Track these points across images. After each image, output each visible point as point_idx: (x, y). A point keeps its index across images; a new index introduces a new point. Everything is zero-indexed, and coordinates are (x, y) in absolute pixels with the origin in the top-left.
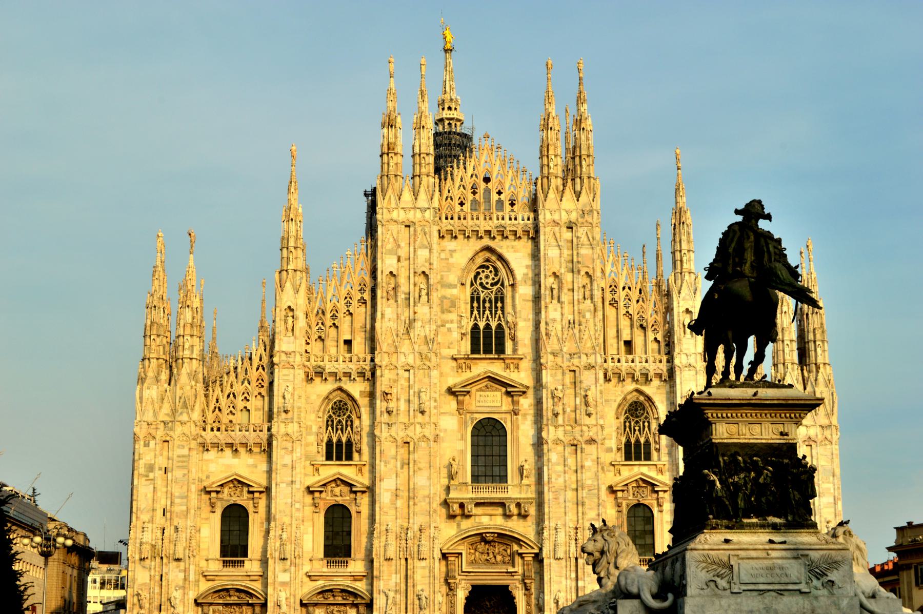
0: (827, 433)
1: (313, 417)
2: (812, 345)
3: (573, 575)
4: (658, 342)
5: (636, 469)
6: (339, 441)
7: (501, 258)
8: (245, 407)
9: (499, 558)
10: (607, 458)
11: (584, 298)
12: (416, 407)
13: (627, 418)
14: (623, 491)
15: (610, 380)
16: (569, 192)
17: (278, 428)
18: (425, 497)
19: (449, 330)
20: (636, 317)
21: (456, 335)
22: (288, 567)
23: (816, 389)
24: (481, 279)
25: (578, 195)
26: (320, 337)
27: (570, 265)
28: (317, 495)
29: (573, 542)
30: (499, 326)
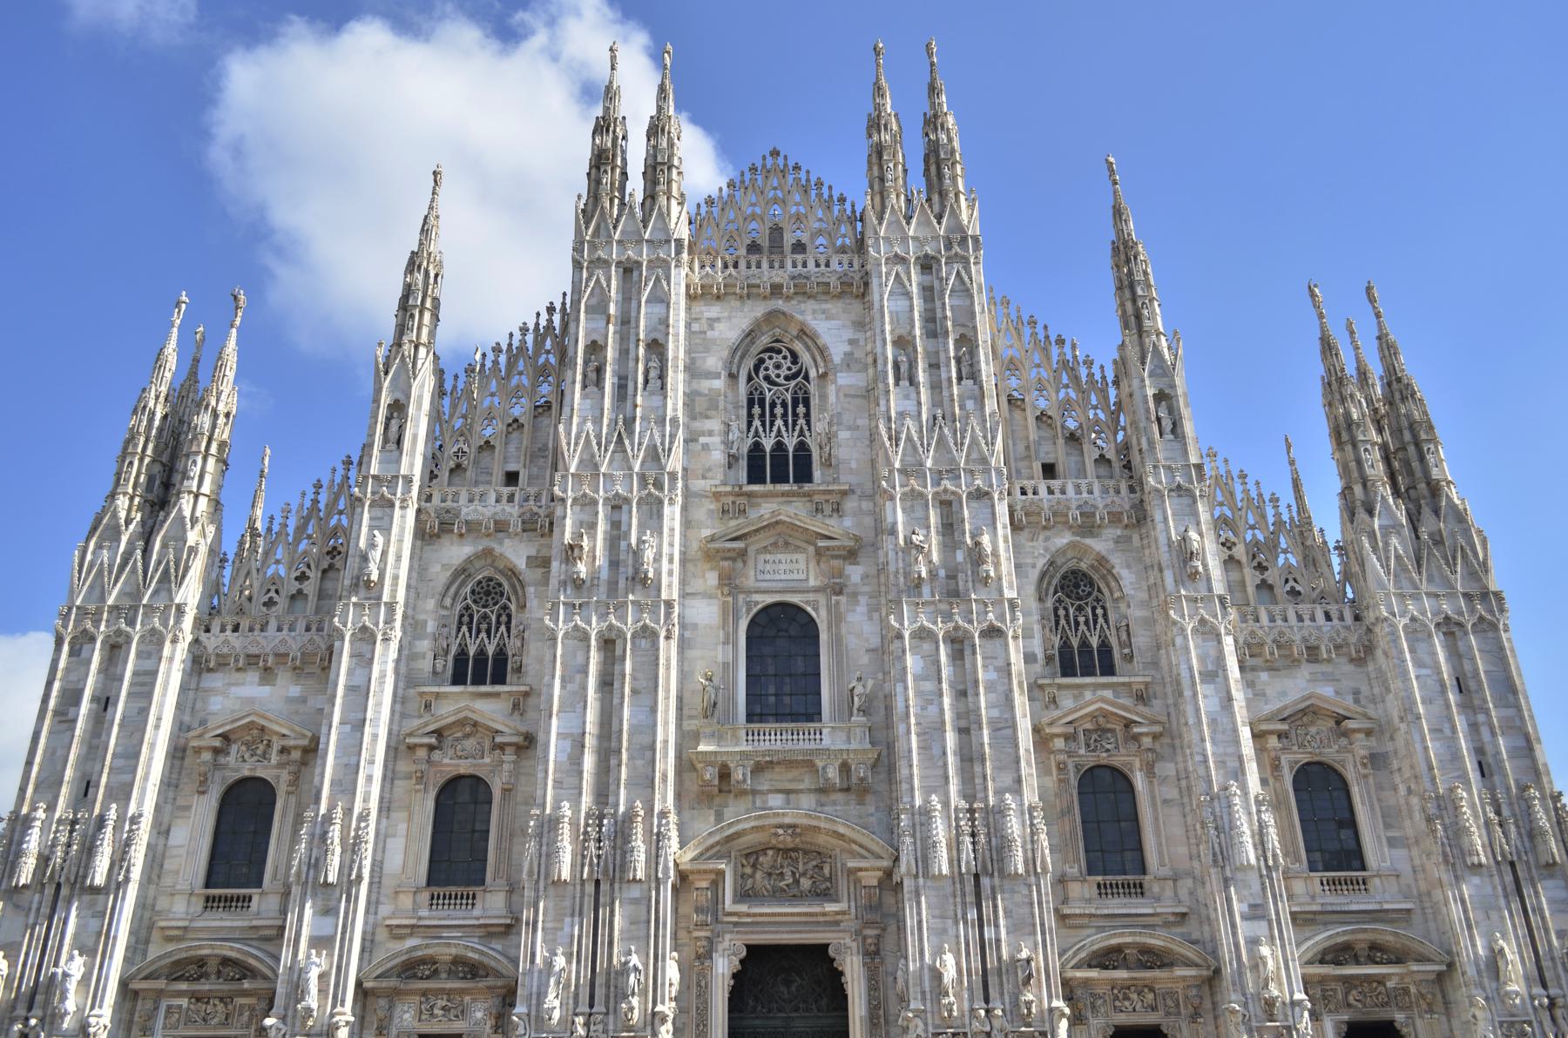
1: (431, 604)
3: (972, 914)
4: (1109, 461)
5: (1088, 695)
6: (481, 652)
7: (804, 334)
8: (300, 592)
9: (806, 883)
11: (960, 379)
12: (630, 571)
13: (1059, 601)
14: (1067, 737)
15: (1021, 529)
17: (348, 619)
18: (643, 748)
19: (706, 447)
21: (718, 456)
22: (332, 904)
24: (767, 369)
26: (458, 466)
27: (931, 326)
28: (422, 753)
29: (968, 839)
30: (802, 447)
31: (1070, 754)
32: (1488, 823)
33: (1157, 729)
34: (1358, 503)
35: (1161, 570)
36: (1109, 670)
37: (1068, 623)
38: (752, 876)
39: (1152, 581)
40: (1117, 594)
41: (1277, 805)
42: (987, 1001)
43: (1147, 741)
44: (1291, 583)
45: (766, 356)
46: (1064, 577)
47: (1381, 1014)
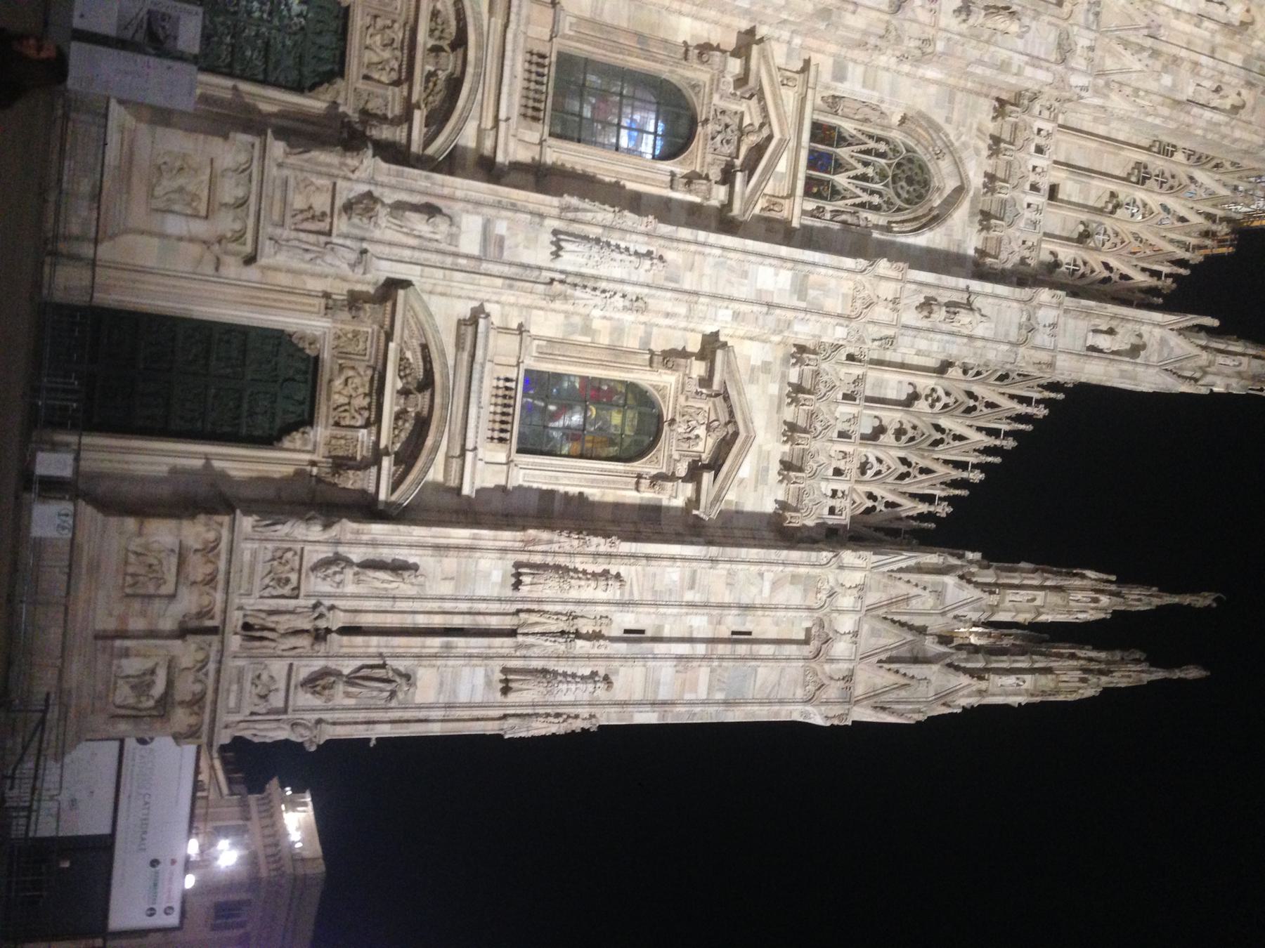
0: (833, 692)
2: (1023, 662)
10: (824, 63)
13: (895, 151)
20: (1108, 222)
23: (935, 667)
31: (716, 83)
32: (572, 617)
37: (868, 152)
40: (896, 228)
41: (616, 353)
43: (720, 193)
44: (876, 467)
46: (922, 168)
47: (323, 410)
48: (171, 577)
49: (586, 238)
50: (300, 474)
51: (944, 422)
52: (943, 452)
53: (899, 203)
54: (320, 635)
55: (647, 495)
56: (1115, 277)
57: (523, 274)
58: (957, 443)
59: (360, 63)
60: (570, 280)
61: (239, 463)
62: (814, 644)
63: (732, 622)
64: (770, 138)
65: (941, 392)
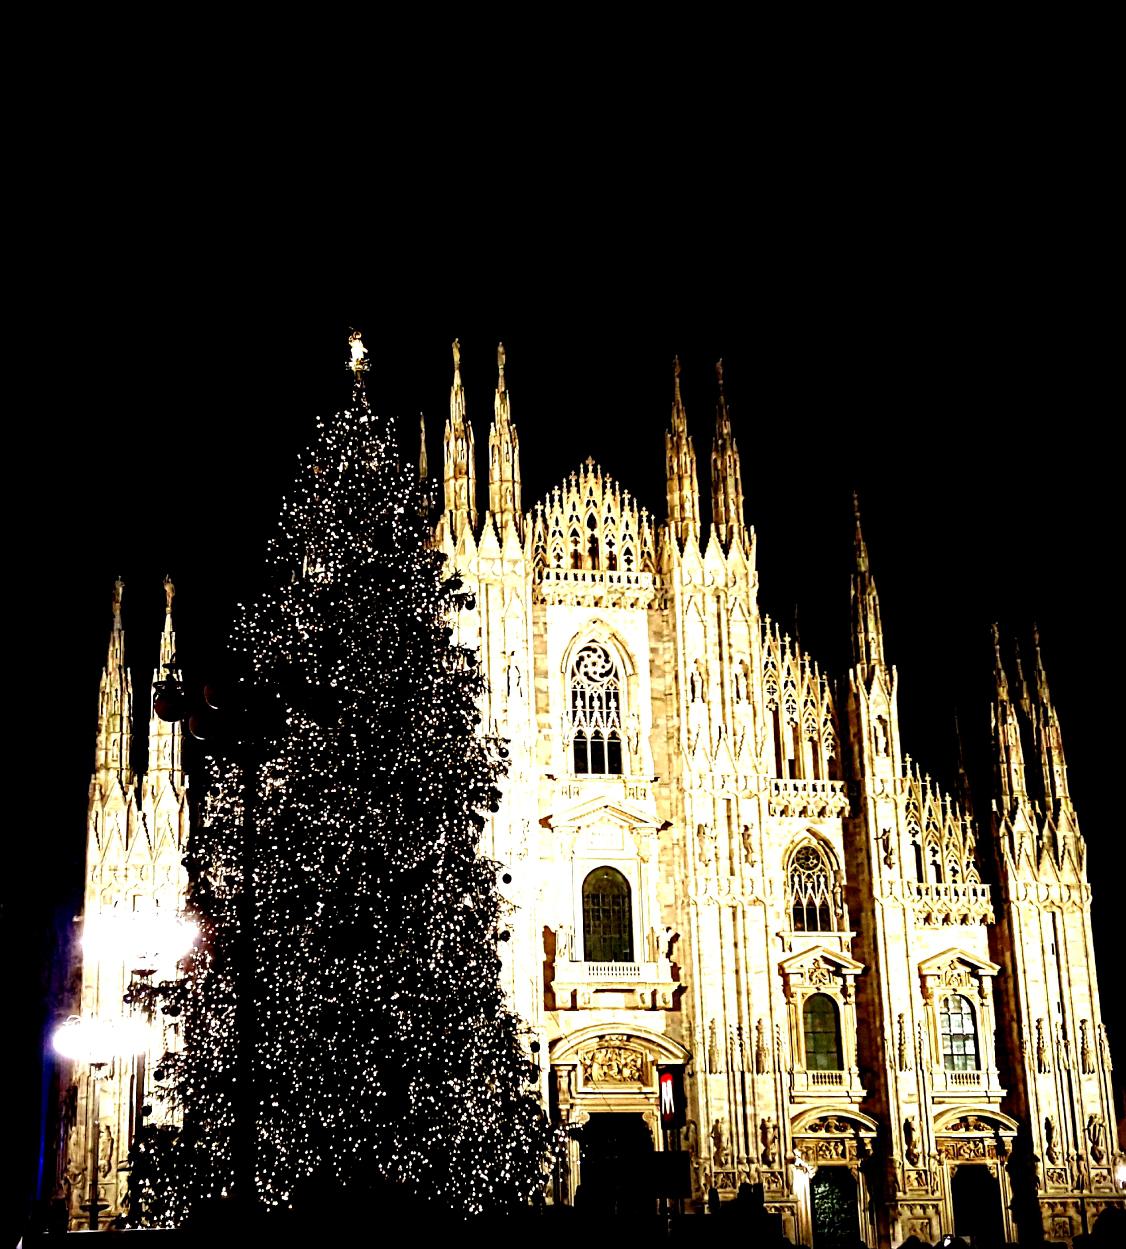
9: (626, 1072)
13: (795, 870)
16: (713, 544)
20: (804, 727)
23: (1057, 833)
25: (726, 548)
29: (737, 1048)
30: (614, 735)
33: (859, 972)
34: (1005, 812)
35: (869, 858)
36: (826, 927)
38: (591, 1066)
39: (859, 860)
40: (835, 868)
42: (747, 1152)
43: (850, 981)
44: (953, 864)
45: (585, 654)
46: (799, 852)
48: (1063, 1219)
49: (901, 1056)
50: (1008, 1169)
51: (924, 823)
52: (939, 825)
53: (820, 865)
54: (1080, 1158)
55: (990, 1001)
56: (830, 717)
57: (920, 1083)
58: (933, 813)
59: (838, 1159)
60: (919, 1061)
61: (1007, 1194)
62: (1055, 909)
63: (1051, 959)
64: (822, 957)
65: (910, 828)
